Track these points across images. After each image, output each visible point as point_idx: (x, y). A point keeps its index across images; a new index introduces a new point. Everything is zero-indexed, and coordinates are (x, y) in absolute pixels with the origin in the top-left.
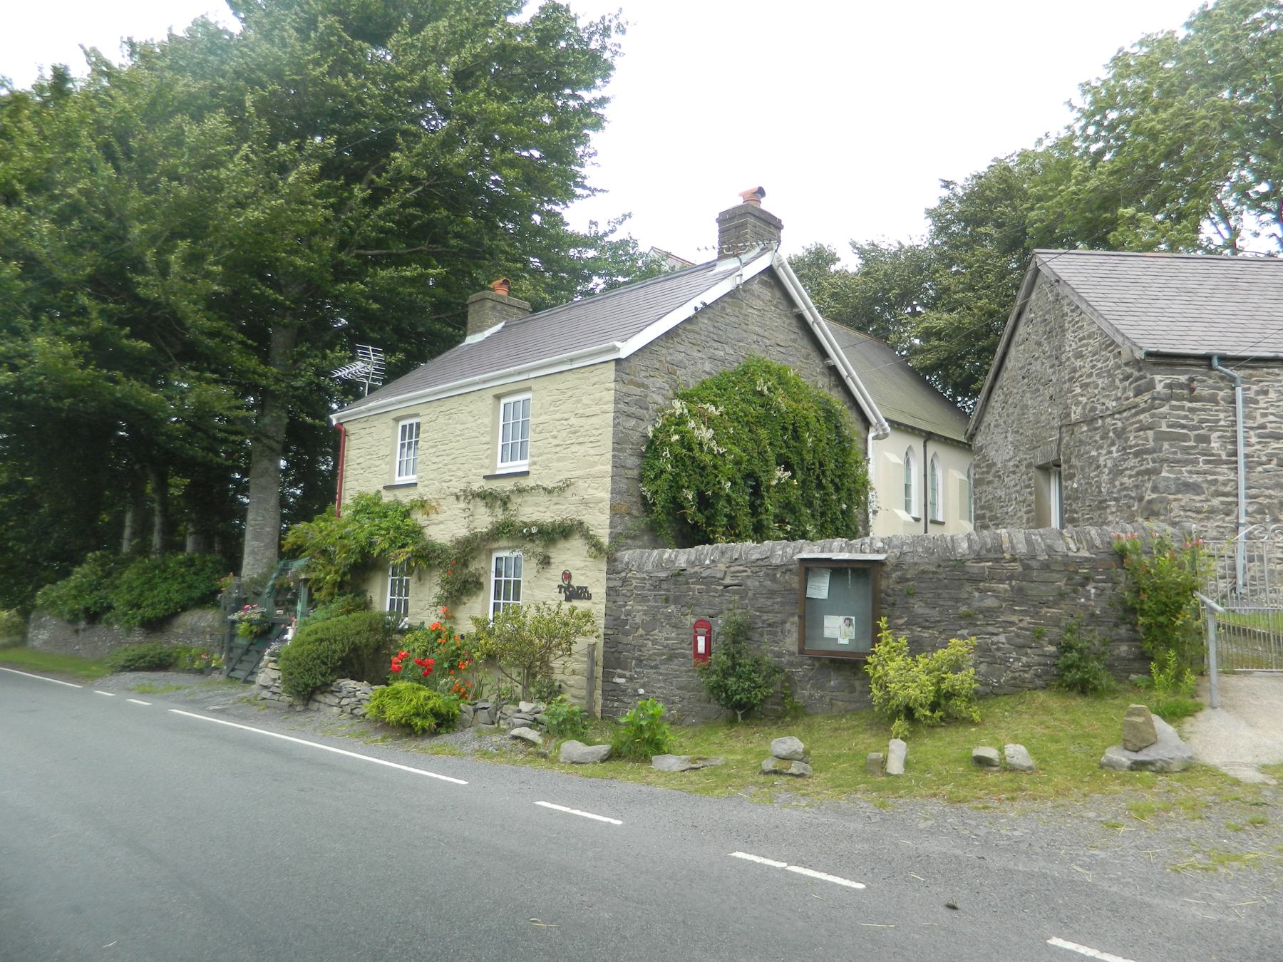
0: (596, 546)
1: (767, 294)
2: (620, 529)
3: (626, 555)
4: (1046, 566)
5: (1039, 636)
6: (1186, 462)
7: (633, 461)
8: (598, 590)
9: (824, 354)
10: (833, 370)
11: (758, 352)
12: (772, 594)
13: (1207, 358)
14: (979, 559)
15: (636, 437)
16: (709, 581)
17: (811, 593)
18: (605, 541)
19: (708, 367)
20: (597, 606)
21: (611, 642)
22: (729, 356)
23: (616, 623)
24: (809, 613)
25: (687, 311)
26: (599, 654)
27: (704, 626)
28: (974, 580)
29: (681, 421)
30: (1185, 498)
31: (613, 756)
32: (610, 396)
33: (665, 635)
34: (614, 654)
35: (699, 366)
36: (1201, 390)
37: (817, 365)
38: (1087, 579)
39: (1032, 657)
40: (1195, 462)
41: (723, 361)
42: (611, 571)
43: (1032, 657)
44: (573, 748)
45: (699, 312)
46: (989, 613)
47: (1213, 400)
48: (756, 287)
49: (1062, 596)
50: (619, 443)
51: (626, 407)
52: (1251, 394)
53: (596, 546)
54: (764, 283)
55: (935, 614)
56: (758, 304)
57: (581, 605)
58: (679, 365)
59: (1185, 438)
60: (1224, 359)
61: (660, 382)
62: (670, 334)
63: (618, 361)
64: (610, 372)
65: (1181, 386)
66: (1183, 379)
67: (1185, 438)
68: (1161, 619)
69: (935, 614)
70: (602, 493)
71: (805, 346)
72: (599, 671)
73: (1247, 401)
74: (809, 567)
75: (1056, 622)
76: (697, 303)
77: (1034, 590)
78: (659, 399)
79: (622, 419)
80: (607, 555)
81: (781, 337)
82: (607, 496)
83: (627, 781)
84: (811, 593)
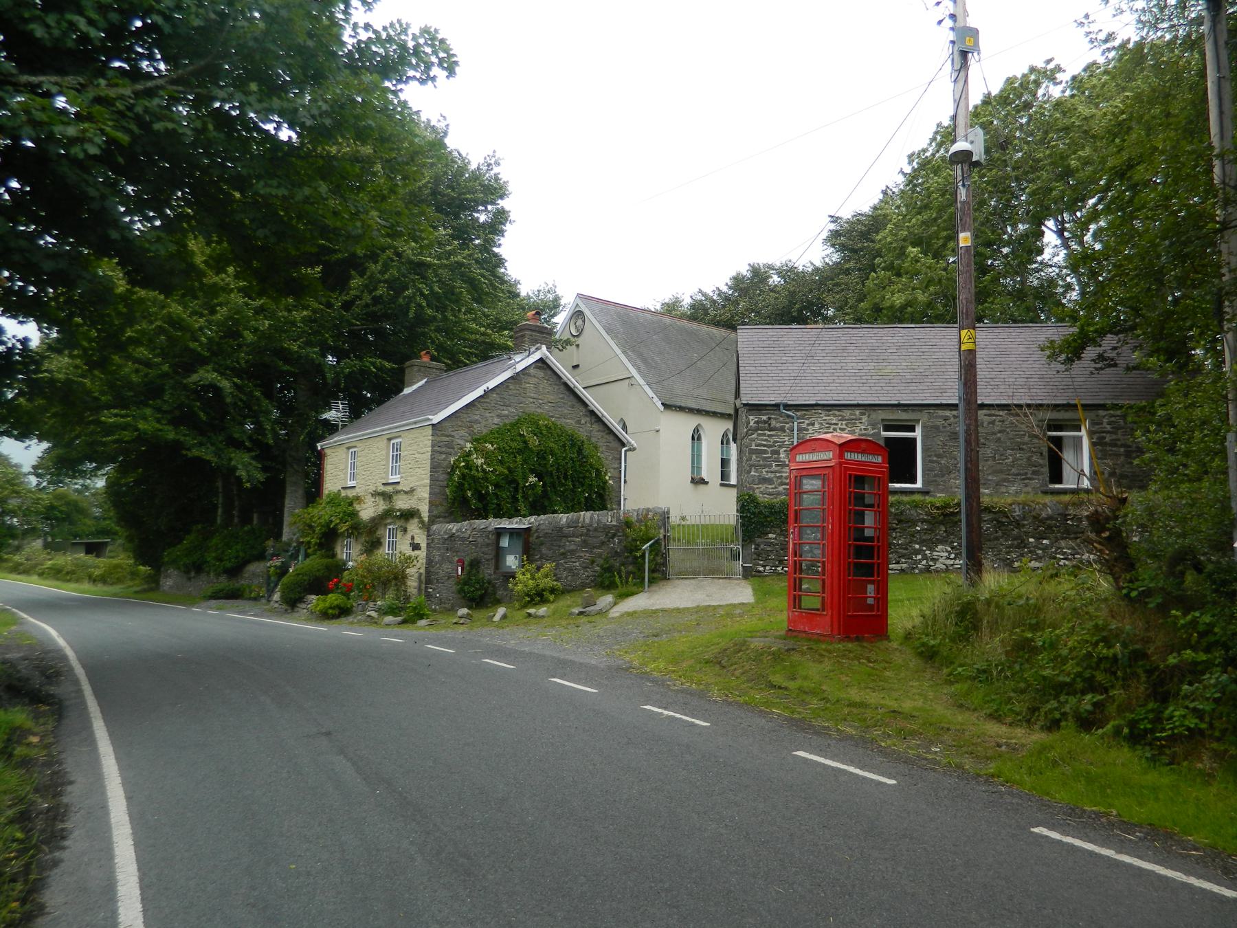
0: (422, 522)
1: (540, 374)
2: (435, 512)
3: (434, 527)
4: (596, 530)
5: (593, 562)
6: (765, 466)
7: (443, 477)
8: (423, 545)
9: (585, 405)
10: (592, 413)
11: (532, 409)
12: (488, 545)
13: (777, 406)
14: (569, 527)
15: (445, 464)
16: (463, 539)
17: (502, 544)
18: (426, 519)
19: (496, 420)
20: (422, 554)
21: (428, 571)
22: (511, 413)
23: (430, 562)
24: (499, 554)
25: (479, 392)
26: (423, 577)
27: (461, 562)
28: (566, 536)
29: (469, 454)
30: (763, 487)
31: (404, 622)
32: (429, 443)
33: (447, 567)
34: (428, 579)
35: (491, 420)
36: (773, 423)
37: (581, 411)
38: (614, 535)
39: (589, 572)
40: (771, 466)
41: (507, 416)
42: (428, 535)
43: (589, 572)
44: (389, 619)
45: (486, 392)
46: (572, 552)
47: (782, 429)
48: (532, 371)
49: (603, 543)
50: (434, 467)
51: (437, 449)
52: (804, 426)
53: (422, 522)
54: (537, 367)
55: (550, 553)
56: (534, 380)
57: (417, 552)
58: (477, 422)
59: (765, 452)
60: (787, 407)
61: (462, 432)
62: (467, 406)
63: (433, 425)
64: (429, 431)
65: (765, 422)
66: (764, 418)
67: (765, 452)
68: (789, 558)
69: (550, 553)
70: (425, 493)
71: (570, 400)
72: (423, 586)
73: (800, 429)
74: (499, 533)
75: (600, 556)
76: (484, 387)
77: (590, 541)
78: (462, 442)
79: (437, 455)
80: (426, 527)
81: (551, 398)
82: (427, 496)
83: (408, 630)
84: (502, 544)
